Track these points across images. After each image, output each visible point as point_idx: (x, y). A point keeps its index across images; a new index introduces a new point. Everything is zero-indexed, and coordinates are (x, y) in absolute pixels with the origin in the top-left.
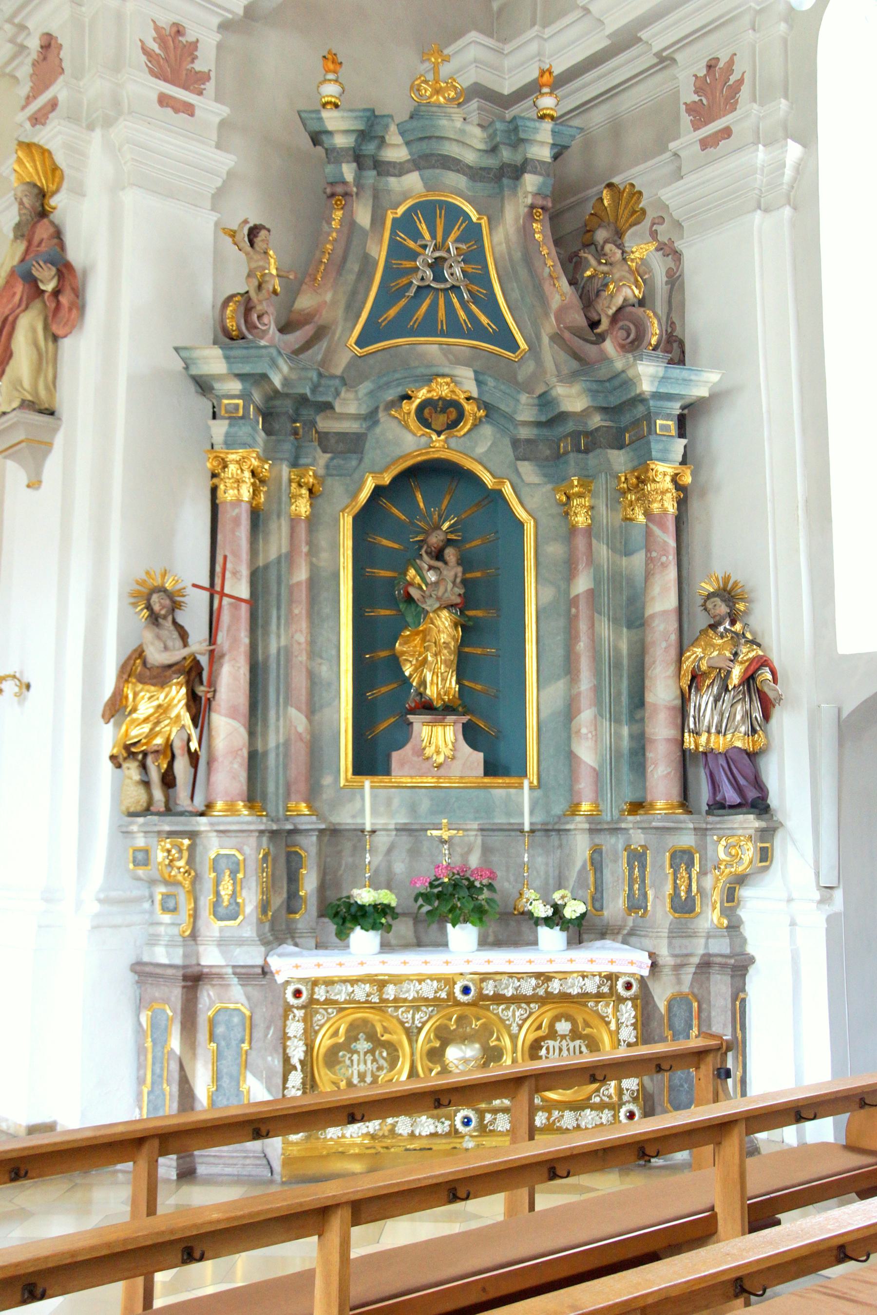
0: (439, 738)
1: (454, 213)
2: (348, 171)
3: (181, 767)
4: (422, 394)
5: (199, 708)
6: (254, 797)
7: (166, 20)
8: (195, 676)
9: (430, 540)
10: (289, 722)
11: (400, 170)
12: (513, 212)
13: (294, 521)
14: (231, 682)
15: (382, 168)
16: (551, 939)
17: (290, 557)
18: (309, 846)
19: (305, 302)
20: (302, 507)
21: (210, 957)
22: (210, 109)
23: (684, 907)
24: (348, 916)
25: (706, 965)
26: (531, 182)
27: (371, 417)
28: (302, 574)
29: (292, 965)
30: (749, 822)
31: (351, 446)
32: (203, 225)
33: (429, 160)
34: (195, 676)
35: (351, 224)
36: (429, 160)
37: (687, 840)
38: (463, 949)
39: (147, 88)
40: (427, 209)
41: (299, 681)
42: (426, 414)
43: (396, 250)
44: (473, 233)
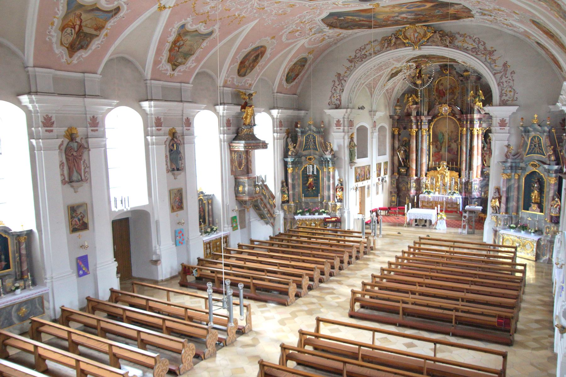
0: (534, 207)
1: (538, 137)
2: (523, 134)
3: (497, 208)
4: (532, 163)
5: (500, 203)
6: (507, 211)
7: (501, 119)
8: (500, 199)
9: (534, 181)
10: (513, 204)
11: (532, 131)
12: (544, 137)
13: (515, 179)
14: (504, 199)
15: (529, 132)
16: (532, 234)
17: (514, 184)
18: (514, 219)
19: (519, 151)
20: (517, 177)
21: (498, 229)
22: (507, 128)
23: (547, 233)
24: (510, 228)
25: (547, 241)
26: (545, 134)
27: (527, 165)
28: (516, 185)
29: (502, 232)
30: (553, 225)
31: (523, 169)
32: (506, 143)
33: (535, 130)
34: (500, 199)
35: (524, 140)
36: (535, 130)
37: (549, 226)
38: (523, 234)
39: (498, 128)
40: (534, 137)
41: (515, 199)
42: (533, 165)
43: (531, 143)
44: (540, 140)
